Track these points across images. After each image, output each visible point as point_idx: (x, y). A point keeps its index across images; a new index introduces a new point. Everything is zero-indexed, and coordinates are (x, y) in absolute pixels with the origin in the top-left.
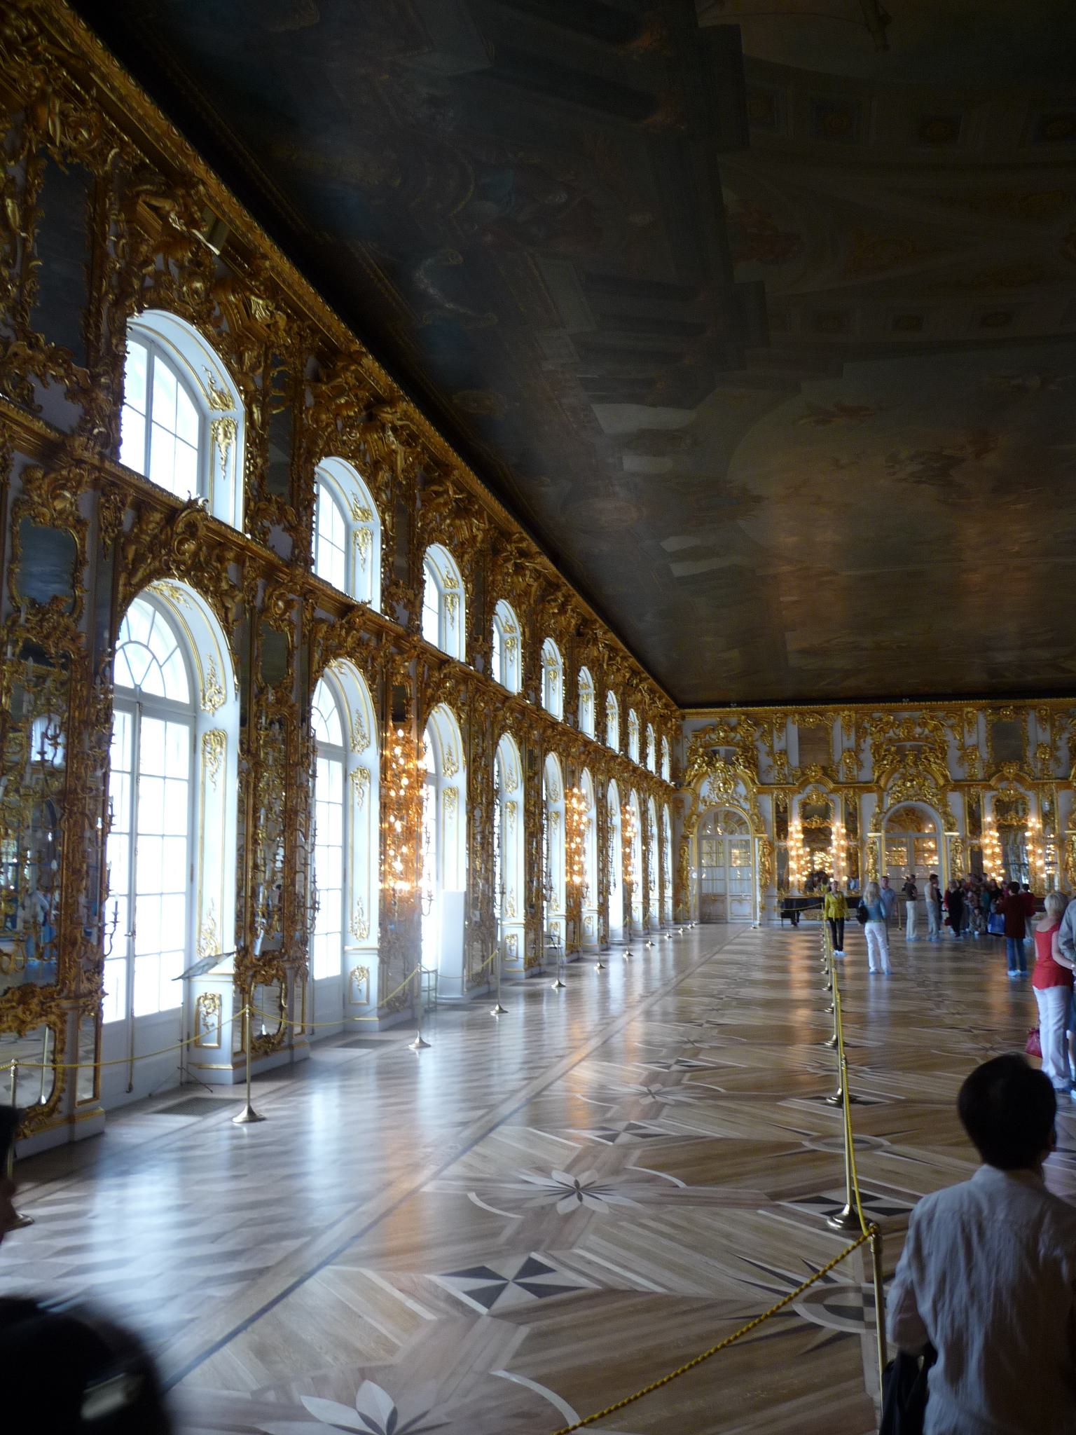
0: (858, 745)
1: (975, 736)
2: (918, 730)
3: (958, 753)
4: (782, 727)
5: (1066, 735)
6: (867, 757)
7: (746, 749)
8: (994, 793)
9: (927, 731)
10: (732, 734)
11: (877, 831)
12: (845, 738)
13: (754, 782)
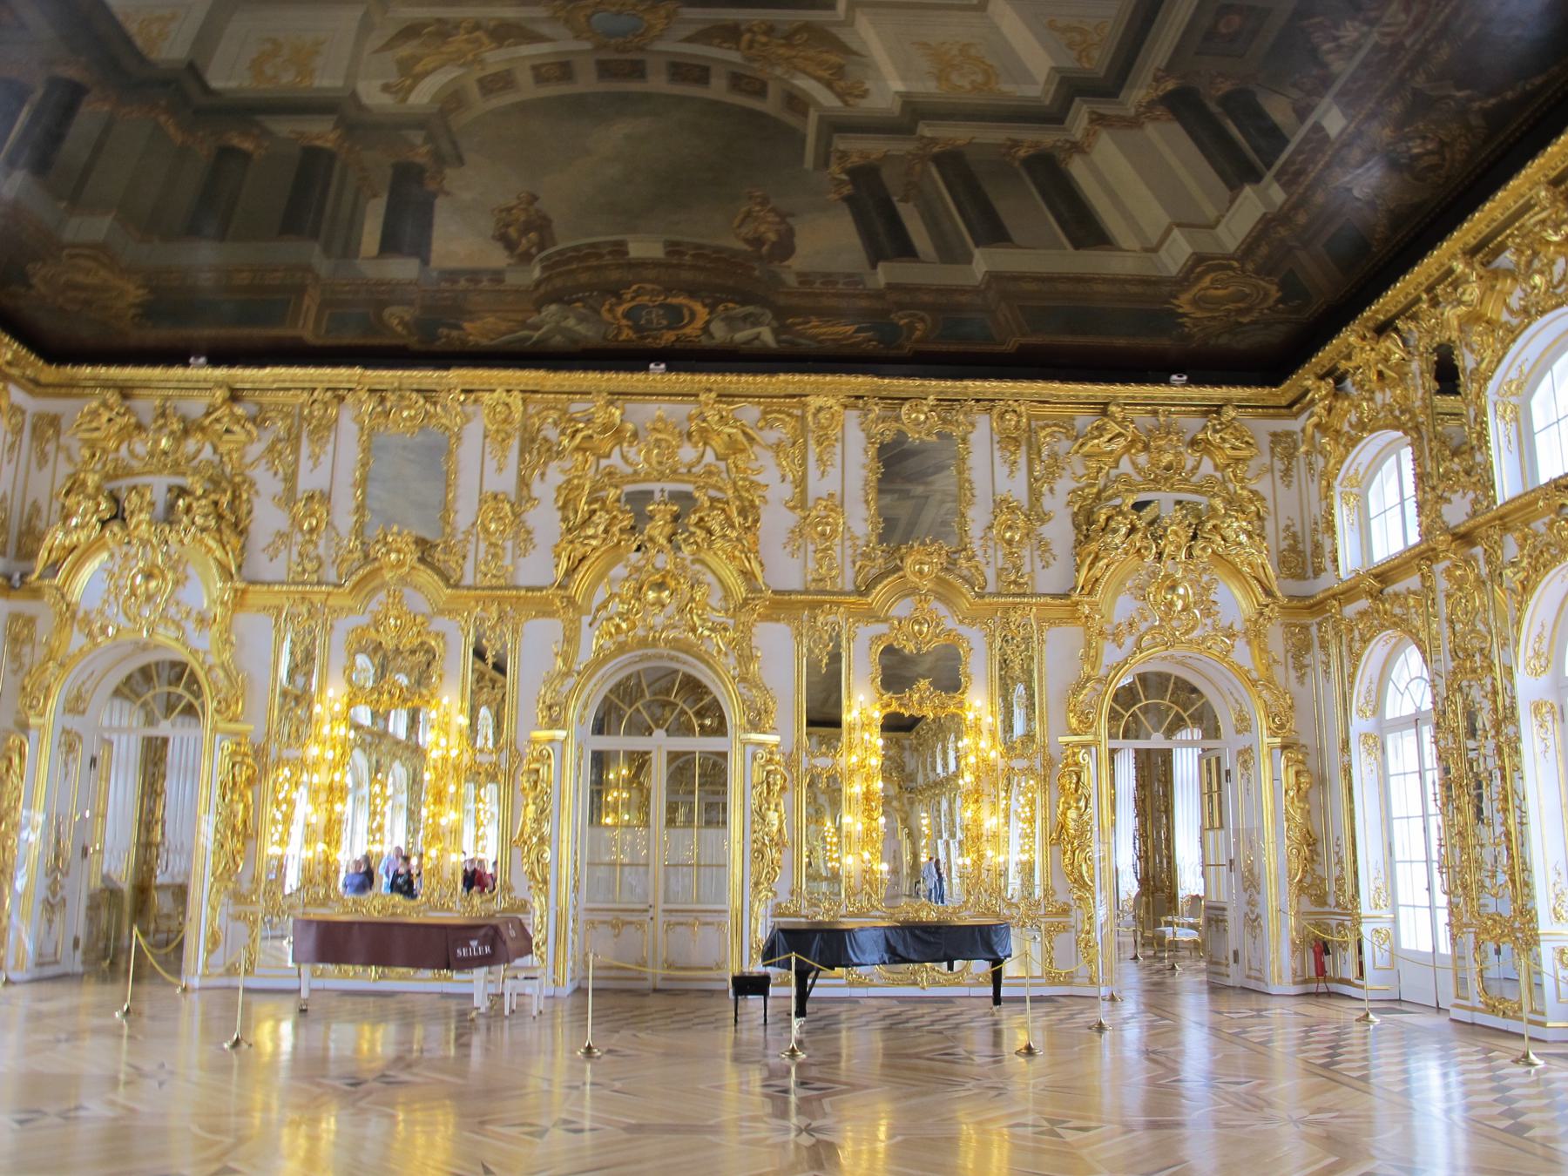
0: (523, 483)
1: (834, 472)
2: (687, 453)
3: (792, 518)
4: (324, 429)
5: (1064, 485)
6: (545, 519)
7: (215, 483)
8: (882, 628)
9: (709, 457)
10: (191, 445)
11: (554, 723)
12: (491, 465)
13: (227, 575)
